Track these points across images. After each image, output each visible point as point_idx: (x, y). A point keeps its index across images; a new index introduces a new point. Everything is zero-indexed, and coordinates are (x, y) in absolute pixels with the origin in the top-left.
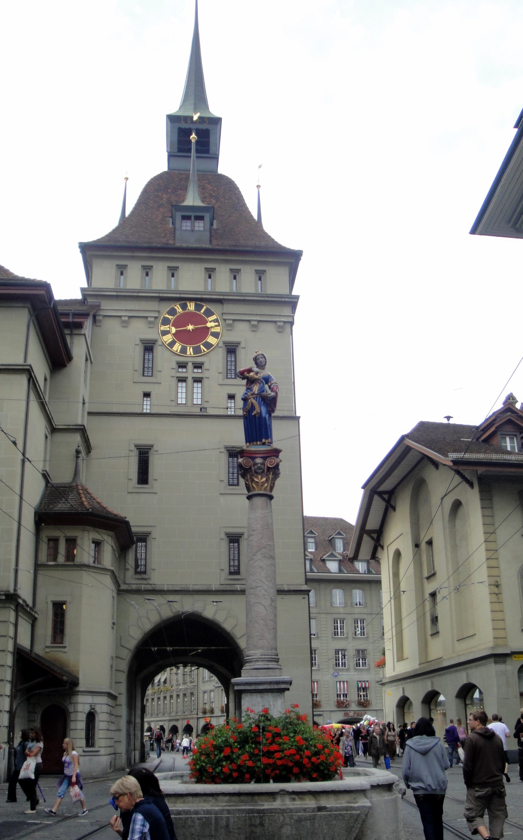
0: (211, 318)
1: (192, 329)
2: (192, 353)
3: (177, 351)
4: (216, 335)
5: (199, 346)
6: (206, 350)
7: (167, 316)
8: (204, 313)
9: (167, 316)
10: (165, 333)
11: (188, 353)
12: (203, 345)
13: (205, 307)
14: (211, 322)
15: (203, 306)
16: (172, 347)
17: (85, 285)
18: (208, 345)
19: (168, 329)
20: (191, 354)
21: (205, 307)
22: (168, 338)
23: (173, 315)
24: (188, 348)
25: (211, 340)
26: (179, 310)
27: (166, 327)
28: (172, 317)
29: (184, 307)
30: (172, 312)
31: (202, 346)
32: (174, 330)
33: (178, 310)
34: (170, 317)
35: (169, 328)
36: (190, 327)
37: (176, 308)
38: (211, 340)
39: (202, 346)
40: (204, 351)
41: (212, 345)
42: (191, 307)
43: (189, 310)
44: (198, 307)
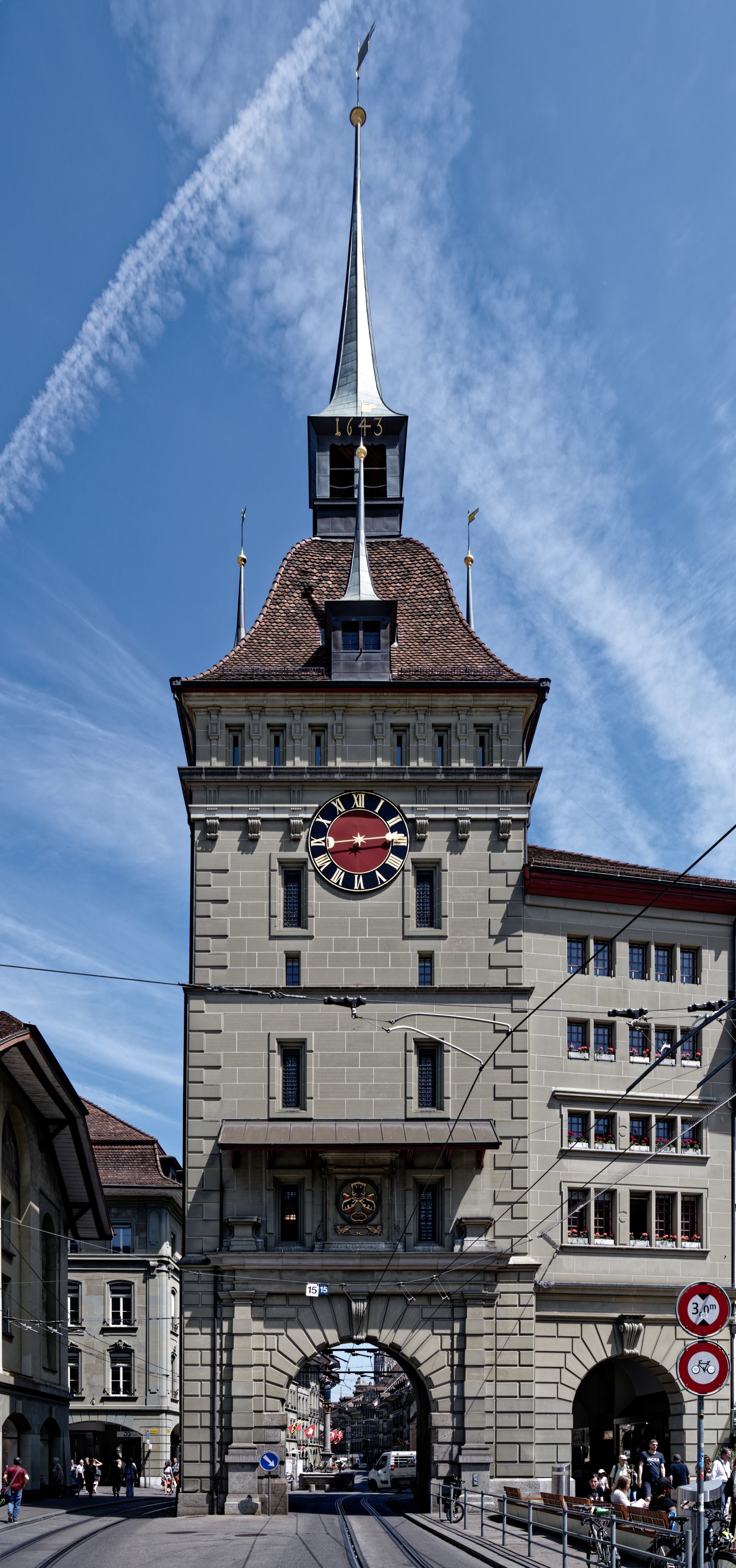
0: (392, 822)
1: (362, 843)
2: (362, 887)
3: (338, 883)
4: (400, 852)
5: (374, 872)
6: (384, 880)
7: (321, 820)
8: (379, 813)
9: (321, 820)
10: (318, 851)
11: (356, 887)
12: (378, 870)
13: (382, 802)
14: (393, 829)
15: (379, 800)
16: (330, 877)
17: (184, 764)
18: (388, 871)
19: (323, 844)
20: (360, 888)
21: (382, 802)
22: (323, 861)
23: (331, 818)
24: (356, 876)
25: (394, 861)
26: (341, 809)
27: (320, 840)
28: (329, 822)
29: (348, 801)
30: (329, 812)
31: (378, 874)
32: (331, 842)
33: (338, 808)
34: (325, 822)
35: (324, 841)
36: (359, 839)
37: (336, 805)
38: (394, 861)
39: (378, 874)
40: (382, 882)
41: (394, 870)
42: (360, 802)
43: (355, 807)
44: (371, 801)
